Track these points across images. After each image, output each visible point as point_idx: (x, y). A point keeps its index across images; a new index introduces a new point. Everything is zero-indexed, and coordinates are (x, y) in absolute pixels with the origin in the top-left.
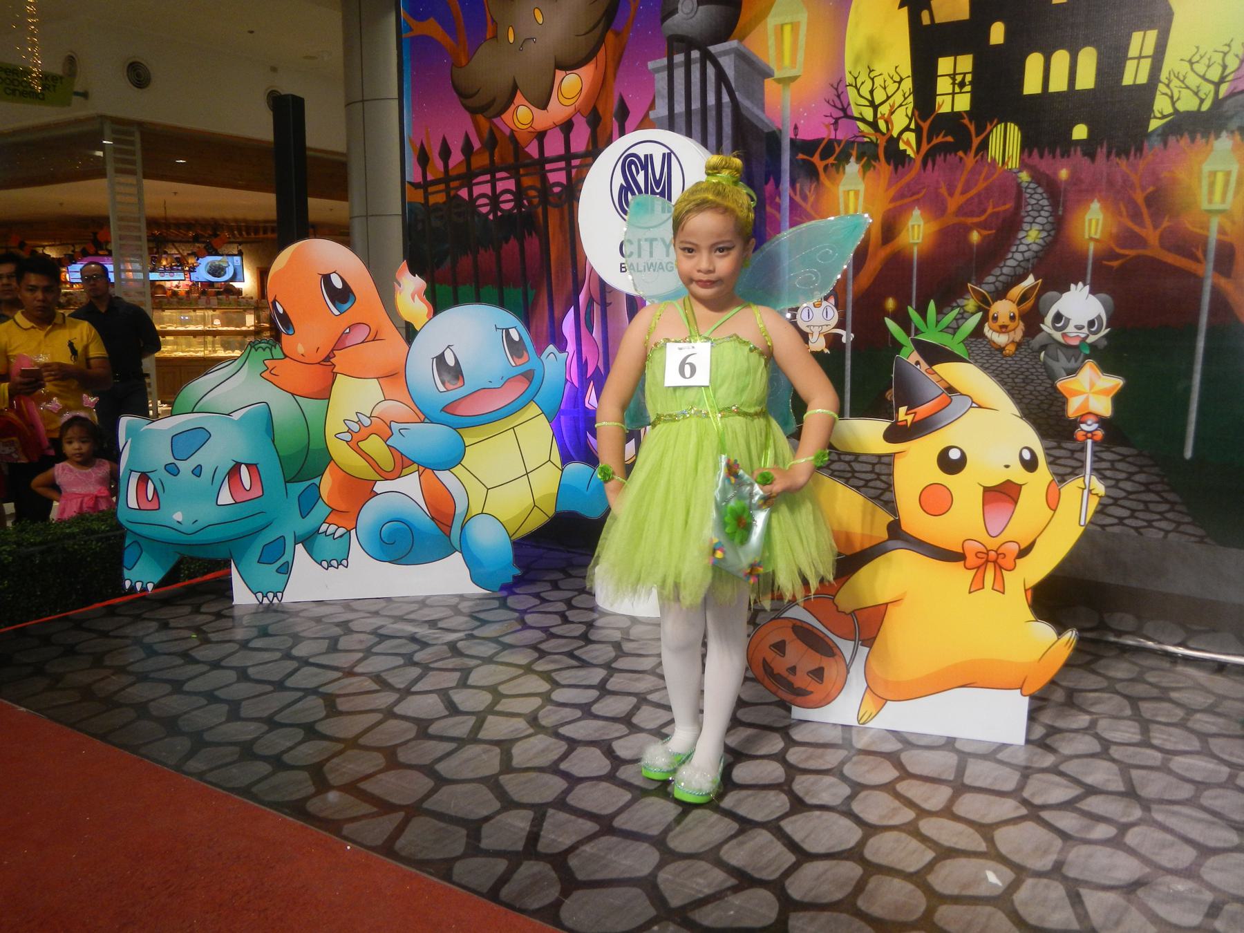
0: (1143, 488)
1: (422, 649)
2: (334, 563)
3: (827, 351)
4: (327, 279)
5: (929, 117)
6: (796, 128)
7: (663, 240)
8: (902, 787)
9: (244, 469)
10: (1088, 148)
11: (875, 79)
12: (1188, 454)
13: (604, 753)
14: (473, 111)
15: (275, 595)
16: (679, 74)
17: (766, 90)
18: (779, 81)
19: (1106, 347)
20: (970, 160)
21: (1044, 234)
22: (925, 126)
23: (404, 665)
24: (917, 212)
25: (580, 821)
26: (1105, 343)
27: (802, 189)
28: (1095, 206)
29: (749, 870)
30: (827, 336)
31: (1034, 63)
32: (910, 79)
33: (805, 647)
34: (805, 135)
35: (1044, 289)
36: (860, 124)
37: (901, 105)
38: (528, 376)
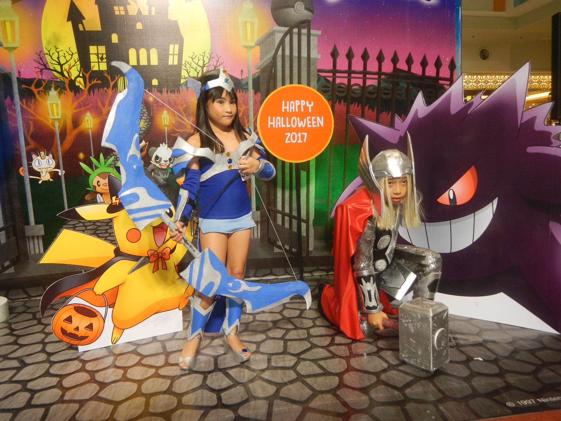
3: (51, 180)
5: (89, 72)
6: (19, 72)
8: (144, 362)
10: (159, 89)
11: (59, 52)
18: (6, 48)
21: (147, 123)
22: (87, 75)
28: (165, 112)
30: (50, 173)
32: (77, 54)
33: (82, 316)
35: (150, 146)
36: (54, 73)
37: (74, 65)
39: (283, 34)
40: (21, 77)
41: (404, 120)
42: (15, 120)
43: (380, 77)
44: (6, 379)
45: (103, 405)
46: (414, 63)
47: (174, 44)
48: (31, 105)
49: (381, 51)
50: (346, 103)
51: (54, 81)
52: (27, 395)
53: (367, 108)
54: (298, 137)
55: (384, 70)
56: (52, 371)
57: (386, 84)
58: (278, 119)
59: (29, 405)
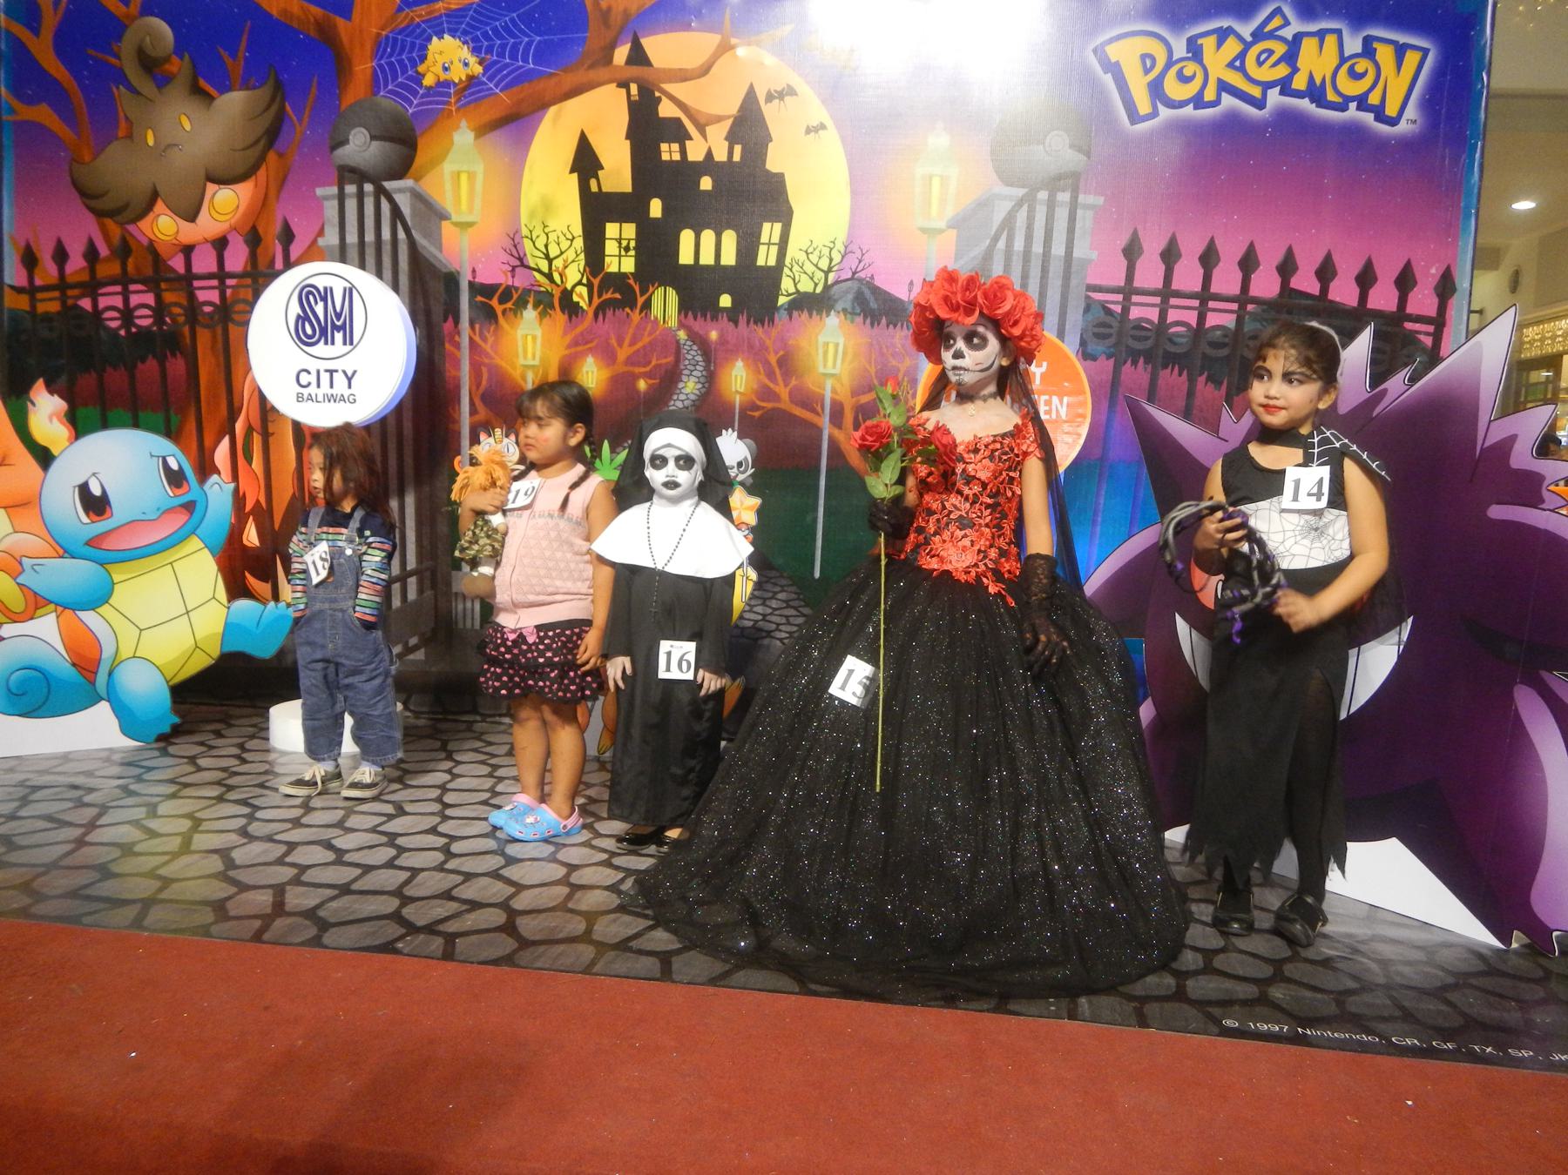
0: (785, 605)
6: (474, 271)
7: (344, 372)
8: (597, 842)
10: (733, 314)
12: (817, 575)
13: (326, 848)
14: (100, 214)
16: (351, 205)
18: (456, 224)
19: (752, 485)
20: (636, 316)
21: (700, 386)
22: (596, 282)
24: (590, 360)
26: (751, 481)
28: (739, 364)
29: (477, 900)
31: (687, 237)
34: (484, 278)
36: (537, 275)
37: (573, 261)
38: (189, 507)
40: (476, 280)
42: (457, 363)
43: (1242, 307)
45: (500, 885)
47: (773, 220)
49: (1252, 245)
50: (1150, 367)
51: (535, 291)
52: (393, 852)
53: (1202, 379)
55: (1255, 291)
56: (441, 829)
59: (390, 864)
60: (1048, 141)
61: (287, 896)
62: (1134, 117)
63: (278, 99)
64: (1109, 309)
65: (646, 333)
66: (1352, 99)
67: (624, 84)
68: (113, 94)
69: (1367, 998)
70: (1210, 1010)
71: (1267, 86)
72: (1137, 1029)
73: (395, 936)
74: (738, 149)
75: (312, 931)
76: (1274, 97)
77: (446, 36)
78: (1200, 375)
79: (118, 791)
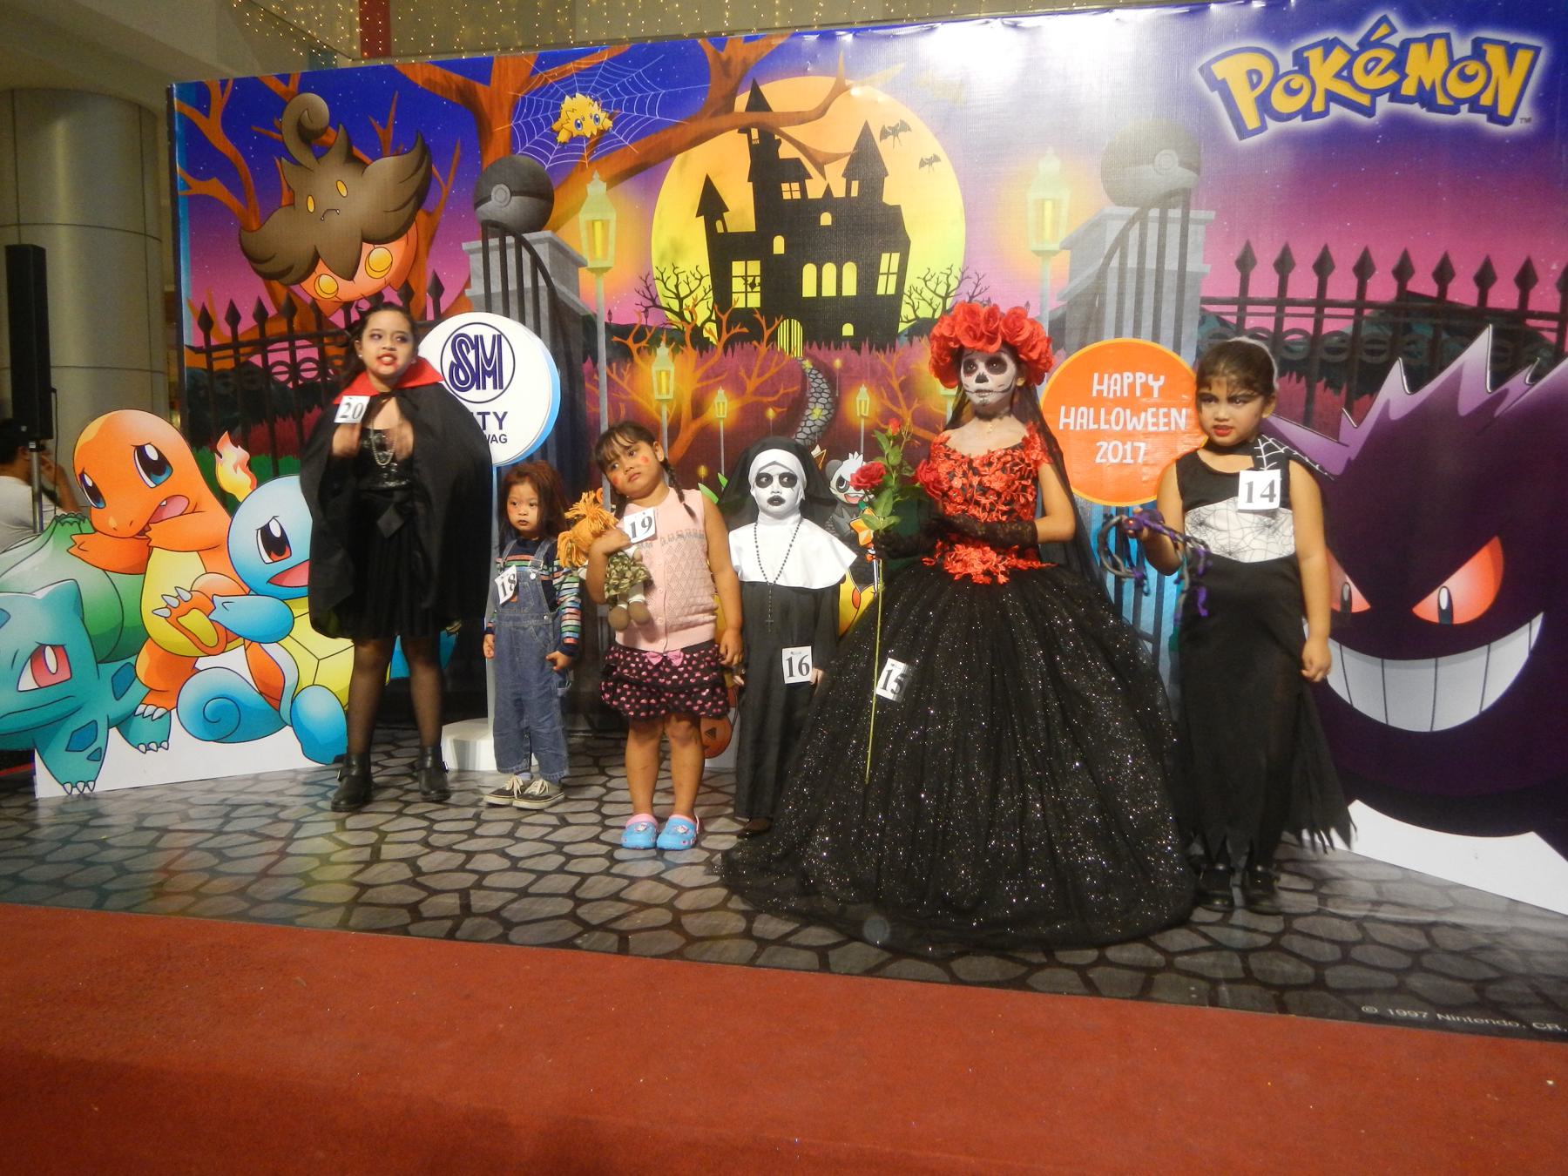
1: (282, 811)
2: (153, 746)
4: (141, 450)
6: (610, 313)
7: (495, 414)
9: (49, 651)
10: (856, 343)
14: (267, 277)
15: (86, 785)
16: (495, 257)
17: (581, 278)
18: (593, 270)
20: (763, 349)
21: (827, 412)
22: (724, 318)
23: (274, 823)
24: (721, 392)
25: (500, 893)
27: (618, 369)
29: (645, 900)
31: (809, 271)
32: (709, 278)
34: (620, 319)
35: (828, 458)
36: (668, 313)
37: (702, 299)
39: (1125, 222)
41: (1359, 422)
43: (1359, 312)
44: (537, 836)
45: (662, 888)
46: (1454, 279)
47: (891, 252)
48: (625, 373)
52: (562, 859)
53: (1320, 385)
54: (1125, 450)
56: (602, 838)
57: (1375, 330)
58: (1082, 414)
59: (561, 870)
60: (1157, 158)
61: (472, 898)
62: (1243, 132)
63: (424, 165)
64: (1224, 320)
65: (775, 361)
66: (1463, 101)
67: (745, 130)
68: (277, 168)
69: (1509, 987)
70: (1349, 997)
71: (1376, 93)
72: (1277, 1014)
73: (575, 932)
74: (855, 185)
75: (499, 930)
76: (1384, 104)
77: (577, 95)
78: (1319, 381)
79: (307, 807)
